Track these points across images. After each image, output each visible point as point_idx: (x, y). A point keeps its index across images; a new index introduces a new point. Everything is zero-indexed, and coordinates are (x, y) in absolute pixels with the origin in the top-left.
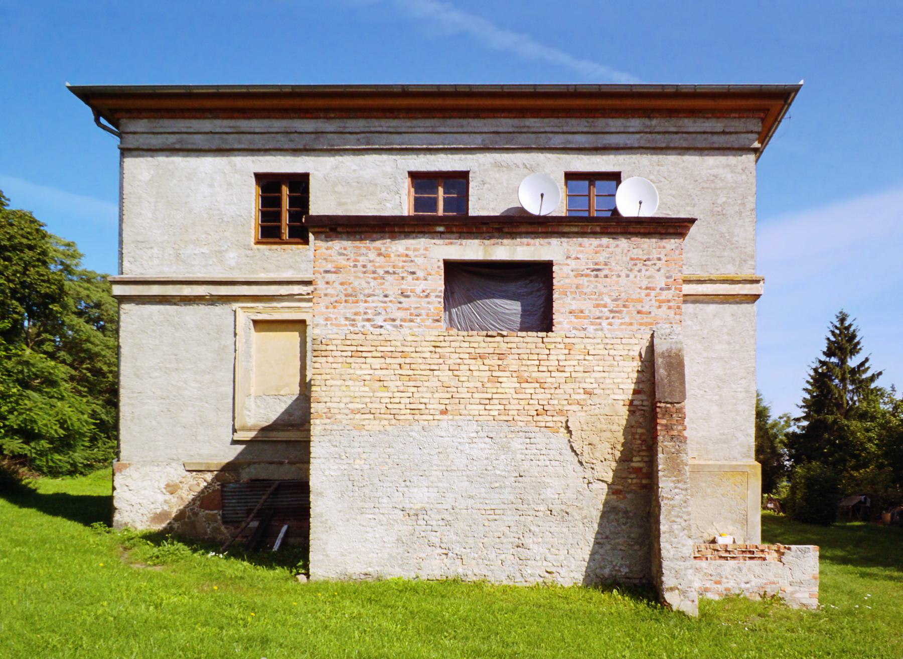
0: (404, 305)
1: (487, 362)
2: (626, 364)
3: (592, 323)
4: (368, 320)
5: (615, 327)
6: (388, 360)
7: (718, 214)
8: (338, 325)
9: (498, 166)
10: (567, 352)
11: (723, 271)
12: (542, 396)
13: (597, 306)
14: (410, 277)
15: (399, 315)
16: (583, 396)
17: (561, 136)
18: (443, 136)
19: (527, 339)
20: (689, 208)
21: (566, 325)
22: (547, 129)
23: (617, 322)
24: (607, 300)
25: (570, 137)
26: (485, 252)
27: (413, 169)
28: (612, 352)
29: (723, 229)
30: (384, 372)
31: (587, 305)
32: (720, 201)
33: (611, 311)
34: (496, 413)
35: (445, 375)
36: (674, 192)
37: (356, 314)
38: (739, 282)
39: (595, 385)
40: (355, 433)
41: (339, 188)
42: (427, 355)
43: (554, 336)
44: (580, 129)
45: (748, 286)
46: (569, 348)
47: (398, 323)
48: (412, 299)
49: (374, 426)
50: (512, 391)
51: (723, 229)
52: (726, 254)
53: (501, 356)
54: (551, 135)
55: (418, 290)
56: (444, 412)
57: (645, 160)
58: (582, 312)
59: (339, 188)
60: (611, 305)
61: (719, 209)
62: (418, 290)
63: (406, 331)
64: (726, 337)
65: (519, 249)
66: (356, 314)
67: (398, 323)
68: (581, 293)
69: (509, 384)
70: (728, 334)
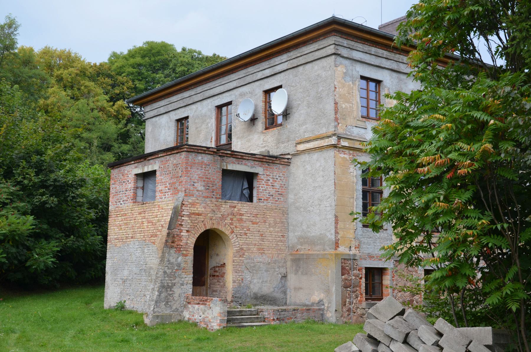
4: (120, 202)
6: (123, 218)
9: (242, 95)
11: (321, 132)
15: (125, 198)
17: (261, 72)
22: (255, 71)
25: (264, 72)
27: (216, 105)
29: (321, 106)
32: (320, 90)
36: (301, 90)
38: (322, 138)
45: (327, 140)
51: (321, 106)
52: (322, 122)
59: (197, 121)
64: (321, 173)
70: (322, 170)
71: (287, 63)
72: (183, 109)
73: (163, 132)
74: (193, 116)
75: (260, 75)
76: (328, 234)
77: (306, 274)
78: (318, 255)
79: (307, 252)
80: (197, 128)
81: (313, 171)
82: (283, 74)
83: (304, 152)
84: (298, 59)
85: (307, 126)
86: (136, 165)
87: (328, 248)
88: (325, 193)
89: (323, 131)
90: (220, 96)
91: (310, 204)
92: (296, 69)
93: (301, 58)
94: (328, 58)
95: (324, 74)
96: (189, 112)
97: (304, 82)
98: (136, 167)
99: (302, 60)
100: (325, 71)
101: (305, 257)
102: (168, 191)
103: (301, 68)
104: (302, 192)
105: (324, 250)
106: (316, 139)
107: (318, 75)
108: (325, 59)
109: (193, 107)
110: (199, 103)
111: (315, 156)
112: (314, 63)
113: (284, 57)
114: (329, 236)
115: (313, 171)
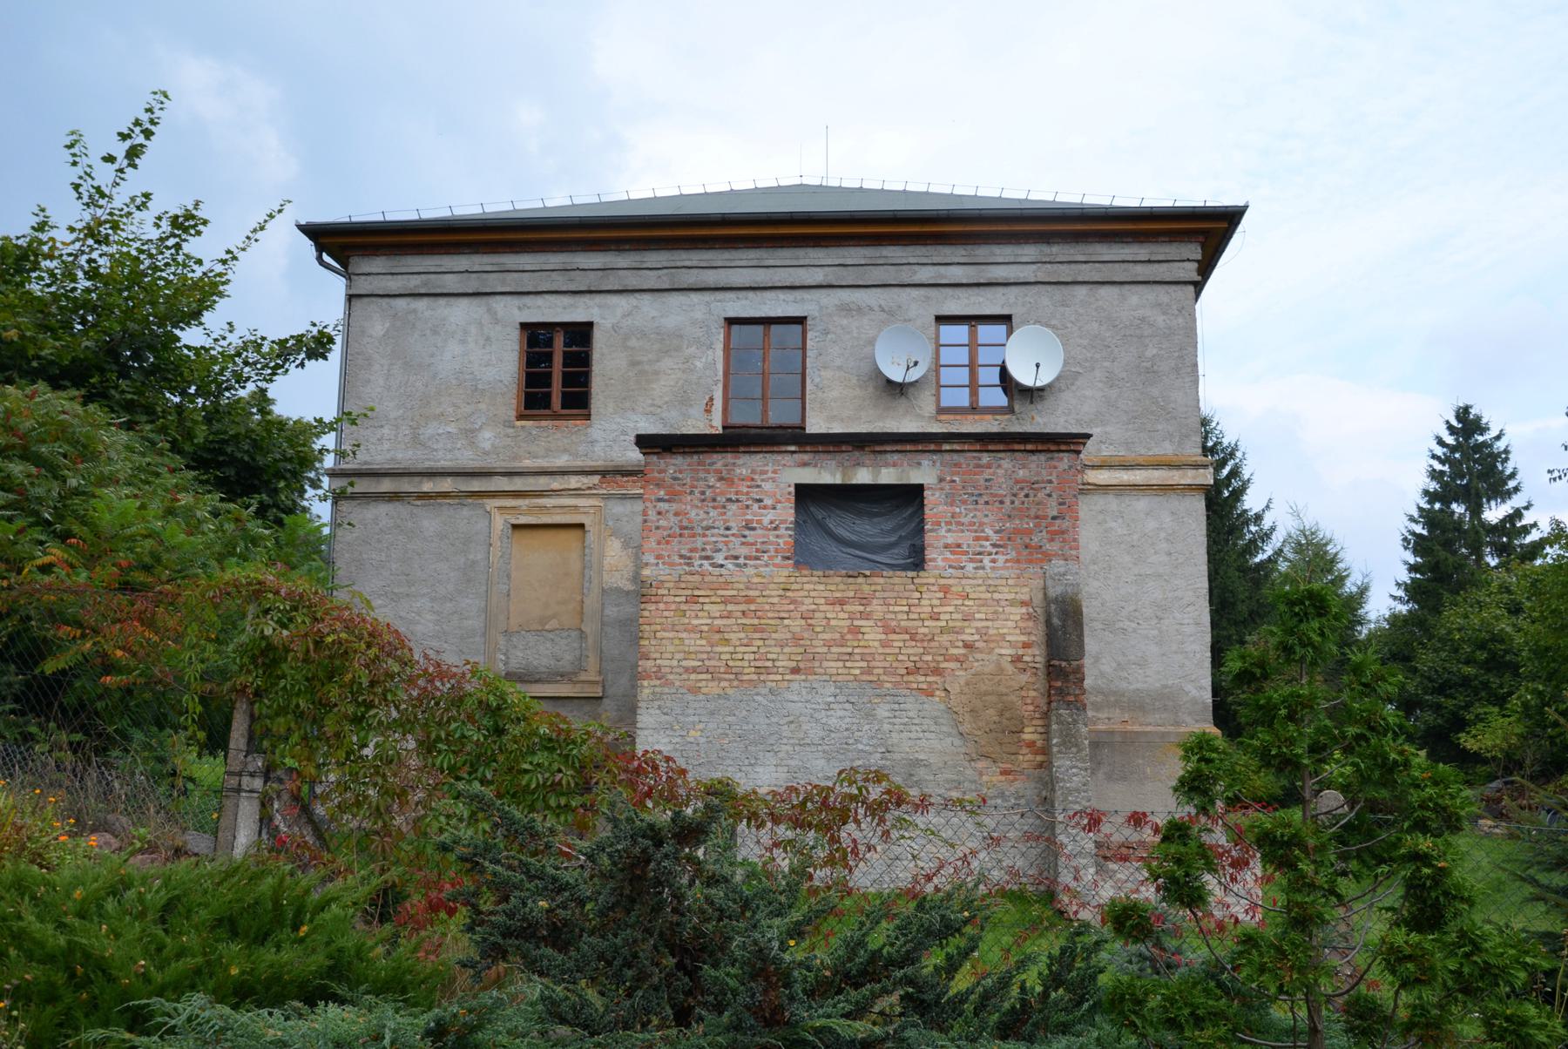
0: (749, 539)
1: (847, 608)
2: (1013, 610)
3: (971, 560)
5: (1000, 564)
6: (730, 607)
7: (1148, 371)
8: (672, 564)
9: (845, 309)
10: (941, 595)
11: (1156, 451)
12: (914, 650)
13: (977, 539)
14: (756, 506)
16: (962, 651)
18: (771, 271)
19: (896, 580)
20: (1106, 364)
21: (940, 563)
22: (912, 260)
23: (1001, 558)
24: (989, 532)
25: (942, 269)
26: (844, 475)
28: (996, 596)
29: (1155, 392)
30: (725, 621)
31: (966, 539)
33: (994, 545)
34: (857, 672)
35: (796, 624)
36: (1085, 342)
37: (691, 550)
38: (1178, 467)
39: (977, 637)
40: (690, 697)
41: (633, 343)
42: (775, 600)
43: (927, 577)
44: (956, 260)
45: (1191, 473)
46: (946, 590)
47: (741, 561)
48: (759, 532)
49: (713, 688)
50: (876, 644)
51: (1155, 392)
53: (864, 600)
54: (916, 268)
55: (766, 521)
56: (795, 671)
57: (1044, 299)
58: (959, 546)
59: (633, 343)
60: (995, 538)
61: (1148, 365)
62: (766, 521)
63: (750, 571)
65: (884, 470)
66: (691, 550)
67: (741, 561)
68: (959, 523)
69: (873, 636)
71: (1034, 267)
72: (566, 300)
73: (454, 348)
74: (615, 328)
75: (924, 275)
76: (1189, 687)
77: (1124, 778)
78: (1164, 735)
79: (1118, 727)
80: (634, 364)
81: (1135, 537)
82: (1014, 290)
83: (1105, 488)
84: (1073, 266)
85: (1109, 429)
86: (806, 457)
87: (1188, 719)
88: (1179, 593)
89: (1167, 449)
90: (751, 294)
91: (1124, 613)
92: (1062, 287)
93: (1084, 266)
94: (1174, 287)
95: (1160, 320)
96: (596, 311)
97: (1095, 325)
98: (805, 464)
99: (1087, 273)
100: (1164, 313)
101: (1118, 738)
102: (989, 549)
103: (1082, 291)
104: (1096, 584)
105: (1177, 724)
106: (1157, 465)
107: (1143, 319)
108: (1166, 287)
109: (622, 303)
110: (647, 297)
111: (1142, 503)
112: (1127, 287)
113: (1029, 251)
114: (1194, 692)
115: (1135, 537)
